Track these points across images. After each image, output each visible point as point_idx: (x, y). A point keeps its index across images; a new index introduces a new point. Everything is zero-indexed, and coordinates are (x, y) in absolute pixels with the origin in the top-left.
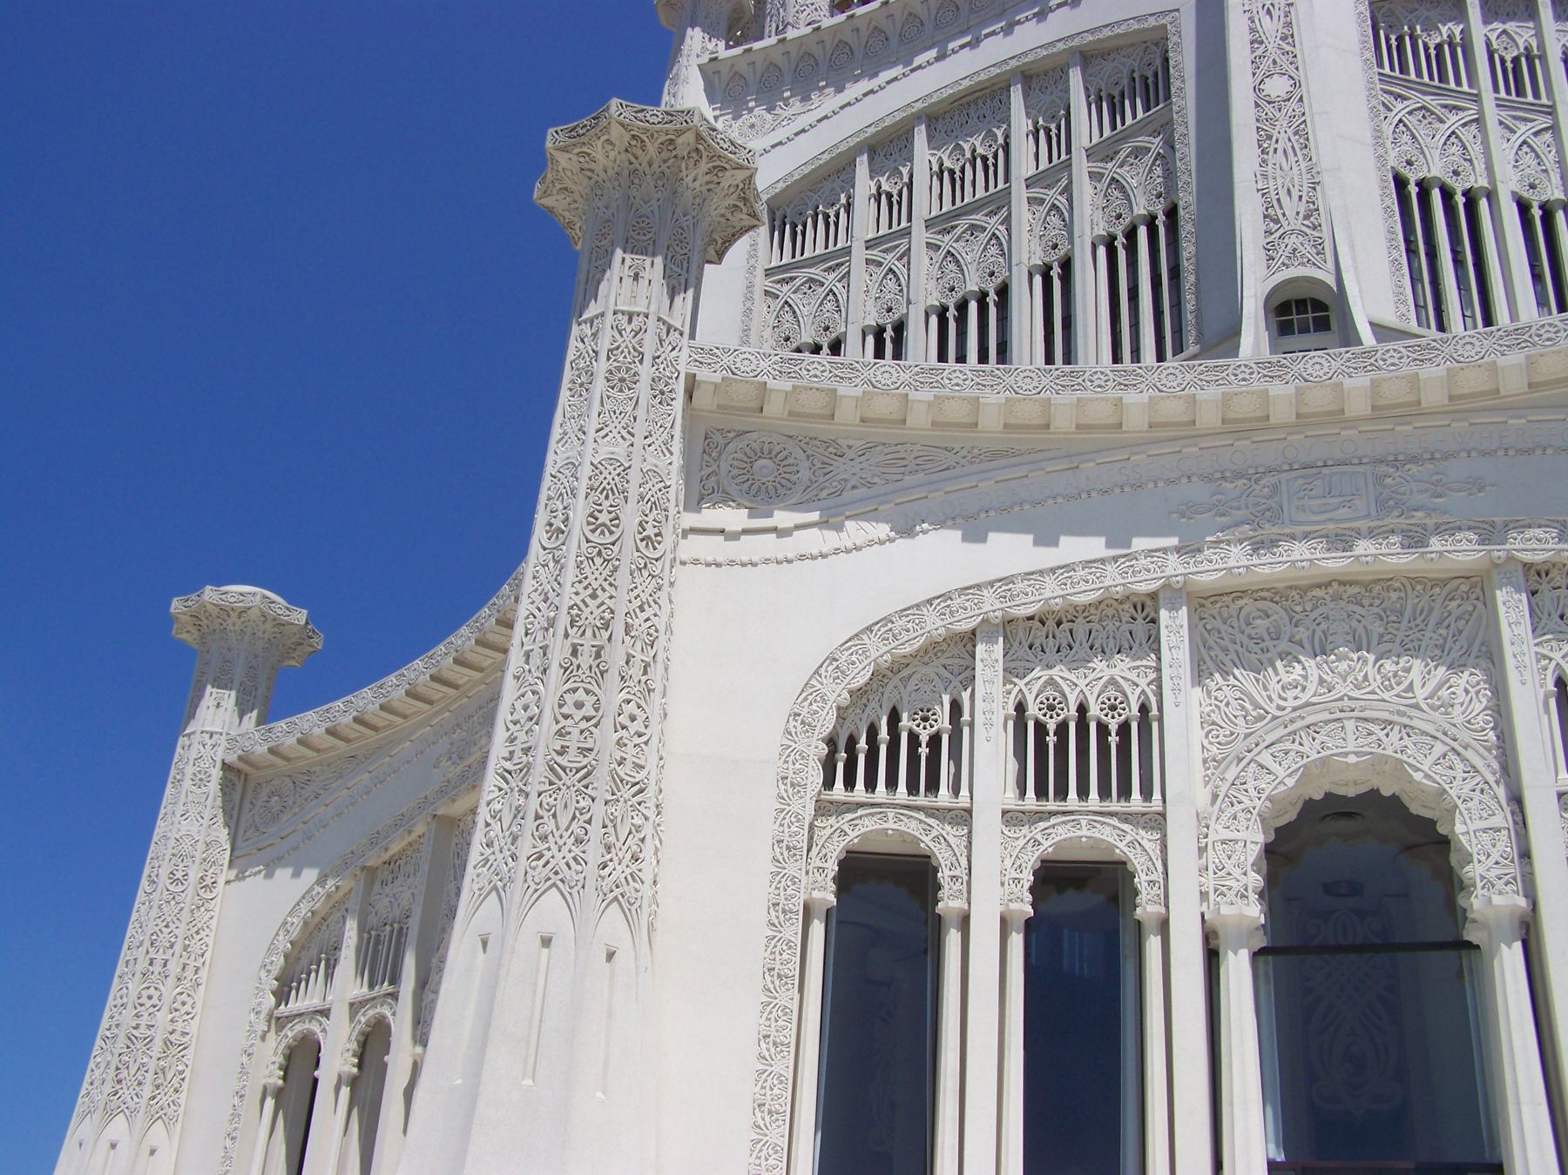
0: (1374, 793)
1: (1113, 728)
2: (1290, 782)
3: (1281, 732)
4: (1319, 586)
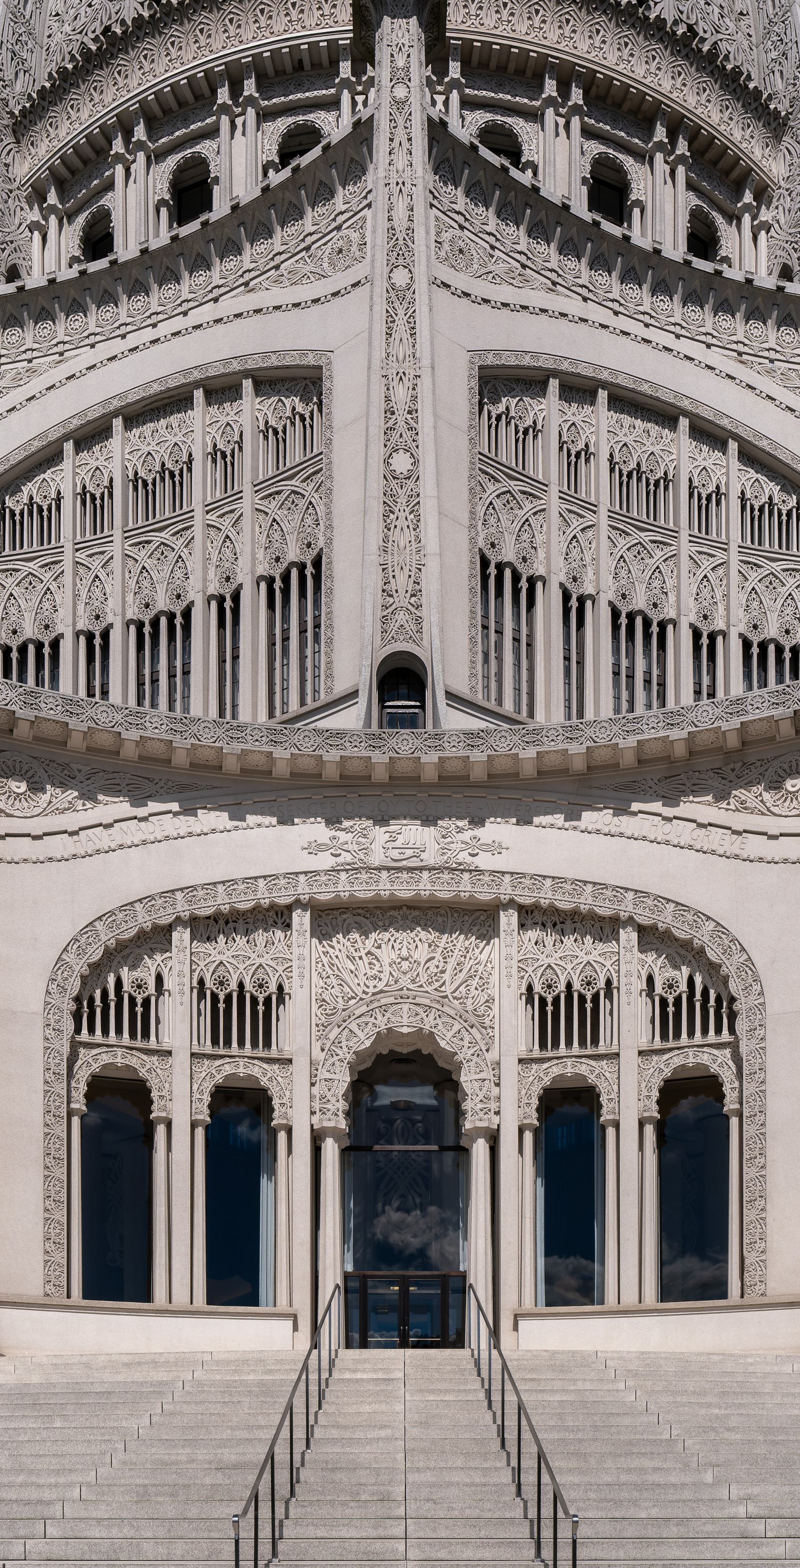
0: (418, 1052)
1: (261, 1000)
2: (368, 1043)
3: (364, 1009)
4: (394, 908)
